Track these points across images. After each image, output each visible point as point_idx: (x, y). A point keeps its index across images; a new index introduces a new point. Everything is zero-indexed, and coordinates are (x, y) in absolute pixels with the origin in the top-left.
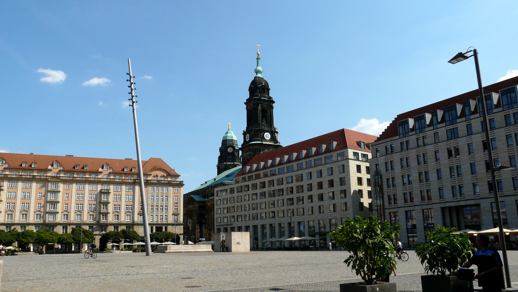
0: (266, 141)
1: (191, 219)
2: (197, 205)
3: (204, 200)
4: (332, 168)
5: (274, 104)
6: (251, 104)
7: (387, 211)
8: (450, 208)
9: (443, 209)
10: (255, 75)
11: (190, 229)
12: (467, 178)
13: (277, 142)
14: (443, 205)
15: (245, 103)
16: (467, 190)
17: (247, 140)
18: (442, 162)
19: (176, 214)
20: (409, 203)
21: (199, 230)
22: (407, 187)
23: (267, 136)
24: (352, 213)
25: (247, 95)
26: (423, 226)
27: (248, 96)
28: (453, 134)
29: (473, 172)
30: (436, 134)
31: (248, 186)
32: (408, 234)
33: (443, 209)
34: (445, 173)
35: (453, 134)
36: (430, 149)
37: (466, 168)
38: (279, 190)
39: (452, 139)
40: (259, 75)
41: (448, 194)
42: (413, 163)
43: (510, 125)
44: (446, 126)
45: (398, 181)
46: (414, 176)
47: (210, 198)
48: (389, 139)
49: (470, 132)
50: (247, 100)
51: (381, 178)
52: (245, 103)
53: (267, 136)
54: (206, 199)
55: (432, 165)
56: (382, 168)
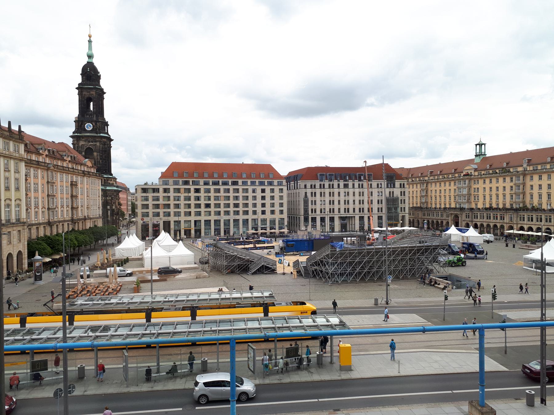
6: (94, 93)
7: (310, 217)
27: (80, 81)
28: (346, 186)
35: (346, 186)
37: (351, 202)
40: (90, 61)
46: (327, 202)
49: (353, 187)
56: (309, 195)
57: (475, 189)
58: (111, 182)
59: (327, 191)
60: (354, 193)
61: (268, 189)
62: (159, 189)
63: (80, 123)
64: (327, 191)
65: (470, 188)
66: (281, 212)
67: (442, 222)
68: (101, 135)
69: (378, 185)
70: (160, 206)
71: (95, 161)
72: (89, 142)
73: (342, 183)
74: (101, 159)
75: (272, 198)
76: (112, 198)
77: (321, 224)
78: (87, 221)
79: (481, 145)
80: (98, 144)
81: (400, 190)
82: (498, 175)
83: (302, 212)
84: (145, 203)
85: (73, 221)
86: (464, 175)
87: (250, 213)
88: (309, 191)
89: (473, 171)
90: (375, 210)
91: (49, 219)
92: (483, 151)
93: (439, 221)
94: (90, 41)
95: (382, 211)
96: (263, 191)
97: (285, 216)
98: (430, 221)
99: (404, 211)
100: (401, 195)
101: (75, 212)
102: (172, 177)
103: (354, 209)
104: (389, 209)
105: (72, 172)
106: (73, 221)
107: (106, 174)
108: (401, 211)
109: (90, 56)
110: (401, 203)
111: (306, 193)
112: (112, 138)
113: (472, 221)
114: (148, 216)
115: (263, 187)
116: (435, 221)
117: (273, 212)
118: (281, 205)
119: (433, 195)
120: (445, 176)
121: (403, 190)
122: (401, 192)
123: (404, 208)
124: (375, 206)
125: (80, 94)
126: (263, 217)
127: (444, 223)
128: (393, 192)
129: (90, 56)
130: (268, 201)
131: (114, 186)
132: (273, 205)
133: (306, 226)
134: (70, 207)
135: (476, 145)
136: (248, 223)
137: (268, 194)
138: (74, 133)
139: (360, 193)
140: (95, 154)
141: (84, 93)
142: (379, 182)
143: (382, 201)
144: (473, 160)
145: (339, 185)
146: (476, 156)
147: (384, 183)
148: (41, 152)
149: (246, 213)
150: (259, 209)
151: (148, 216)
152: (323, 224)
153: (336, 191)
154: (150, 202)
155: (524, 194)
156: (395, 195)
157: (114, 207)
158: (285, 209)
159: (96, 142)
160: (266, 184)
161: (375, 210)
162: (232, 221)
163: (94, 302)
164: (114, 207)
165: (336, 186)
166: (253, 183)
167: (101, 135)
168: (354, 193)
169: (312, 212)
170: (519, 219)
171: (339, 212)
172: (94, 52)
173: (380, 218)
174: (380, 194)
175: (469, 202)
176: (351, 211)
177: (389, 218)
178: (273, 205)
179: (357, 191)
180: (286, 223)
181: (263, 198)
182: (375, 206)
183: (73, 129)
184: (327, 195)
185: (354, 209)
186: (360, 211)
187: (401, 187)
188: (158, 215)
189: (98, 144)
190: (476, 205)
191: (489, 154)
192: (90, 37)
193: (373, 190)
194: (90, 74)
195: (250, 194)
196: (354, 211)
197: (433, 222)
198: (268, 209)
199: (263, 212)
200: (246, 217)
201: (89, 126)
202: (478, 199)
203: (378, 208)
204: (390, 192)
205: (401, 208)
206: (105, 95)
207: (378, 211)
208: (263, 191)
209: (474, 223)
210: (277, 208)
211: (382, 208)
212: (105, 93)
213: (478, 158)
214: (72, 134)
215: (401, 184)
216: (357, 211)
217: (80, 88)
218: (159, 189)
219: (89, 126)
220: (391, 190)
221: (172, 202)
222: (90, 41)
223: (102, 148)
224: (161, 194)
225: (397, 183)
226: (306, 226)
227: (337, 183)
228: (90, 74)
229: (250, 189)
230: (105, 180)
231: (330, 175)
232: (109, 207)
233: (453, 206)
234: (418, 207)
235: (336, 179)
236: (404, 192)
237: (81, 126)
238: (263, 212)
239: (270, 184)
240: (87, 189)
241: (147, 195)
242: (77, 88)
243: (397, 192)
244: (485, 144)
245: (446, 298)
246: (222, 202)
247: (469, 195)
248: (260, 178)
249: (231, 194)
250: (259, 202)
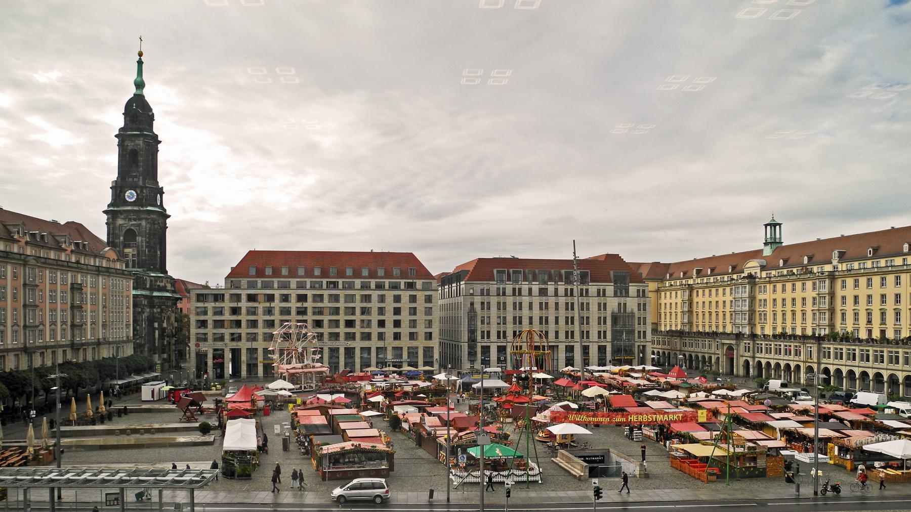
7: (479, 345)
13: (165, 210)
18: (534, 312)
19: (128, 326)
20: (502, 340)
28: (543, 292)
29: (557, 322)
30: (530, 290)
34: (536, 320)
35: (543, 292)
37: (552, 319)
42: (510, 308)
46: (510, 319)
49: (556, 294)
55: (525, 312)
56: (478, 307)
57: (760, 300)
58: (162, 284)
59: (510, 300)
60: (557, 304)
61: (405, 295)
62: (223, 295)
63: (118, 189)
64: (510, 300)
65: (752, 298)
66: (429, 336)
67: (710, 358)
68: (149, 208)
69: (599, 291)
70: (226, 324)
71: (138, 251)
72: (130, 220)
73: (536, 288)
74: (147, 247)
75: (413, 311)
76: (162, 310)
77: (499, 359)
78: (101, 346)
79: (774, 225)
80: (144, 223)
81: (636, 300)
82: (794, 277)
83: (465, 337)
84: (202, 318)
85: (75, 347)
86: (744, 277)
87: (374, 336)
88: (478, 300)
89: (758, 271)
90: (594, 336)
91: (25, 343)
92: (778, 236)
93: (707, 356)
95: (605, 337)
96: (397, 299)
97: (435, 343)
98: (687, 354)
99: (645, 337)
100: (639, 310)
101: (77, 332)
102: (246, 275)
103: (557, 332)
104: (616, 335)
105: (77, 267)
106: (75, 347)
107: (154, 272)
108: (639, 337)
110: (639, 324)
112: (168, 213)
113: (754, 358)
114: (205, 340)
115: (397, 293)
116: (700, 355)
117: (412, 336)
119: (700, 310)
120: (719, 277)
121: (642, 301)
122: (639, 305)
123: (645, 332)
124: (594, 329)
125: (121, 145)
126: (397, 343)
127: (713, 360)
128: (625, 304)
130: (405, 317)
131: (167, 291)
132: (413, 323)
133: (472, 361)
134: (69, 324)
135: (766, 225)
136: (369, 354)
137: (405, 304)
138: (109, 206)
139: (567, 304)
140: (139, 239)
141: (126, 143)
142: (602, 286)
143: (605, 318)
144: (761, 251)
145: (530, 290)
146: (766, 244)
147: (610, 289)
148: (16, 237)
149: (367, 337)
150: (389, 330)
151: (205, 340)
152: (502, 358)
153: (526, 300)
154: (210, 318)
155: (832, 311)
156: (628, 310)
157: (165, 325)
158: (435, 330)
159: (140, 219)
160: (402, 287)
161: (594, 336)
162: (342, 351)
163: (141, 478)
164: (165, 325)
165: (525, 291)
166: (379, 287)
167: (149, 208)
168: (557, 304)
169: (483, 337)
170: (822, 355)
173: (602, 349)
174: (602, 307)
175: (752, 324)
176: (552, 336)
177: (616, 351)
178: (413, 323)
179: (562, 301)
180: (436, 356)
181: (397, 311)
182: (594, 329)
183: (109, 199)
184: (510, 308)
185: (557, 332)
187: (638, 296)
188: (221, 338)
189: (144, 223)
190: (762, 328)
191: (786, 242)
193: (591, 300)
194: (138, 114)
195: (374, 305)
196: (557, 337)
197: (697, 357)
198: (405, 330)
199: (397, 336)
200: (366, 344)
201: (131, 195)
202: (765, 319)
203: (599, 332)
204: (619, 304)
205: (639, 332)
206: (159, 146)
207: (599, 337)
208: (397, 299)
209: (757, 360)
210: (421, 329)
211: (605, 332)
212: (160, 142)
213: (768, 247)
214: (106, 208)
215: (638, 291)
216: (562, 336)
217: (122, 136)
218: (223, 295)
219: (131, 195)
220: (622, 300)
221: (244, 318)
223: (150, 229)
224: (227, 305)
225: (633, 289)
226: (472, 361)
228: (138, 114)
229: (375, 294)
230: (151, 281)
231: (514, 272)
232: (156, 325)
233: (728, 330)
234: (676, 331)
235: (525, 279)
236: (645, 305)
237: (119, 196)
238: (397, 336)
239: (410, 286)
240: (104, 294)
241: (206, 305)
242: (116, 136)
243: (632, 304)
244: (780, 225)
245: (598, 492)
246: (326, 318)
247: (752, 312)
248: (376, 277)
249: (342, 305)
250: (389, 318)
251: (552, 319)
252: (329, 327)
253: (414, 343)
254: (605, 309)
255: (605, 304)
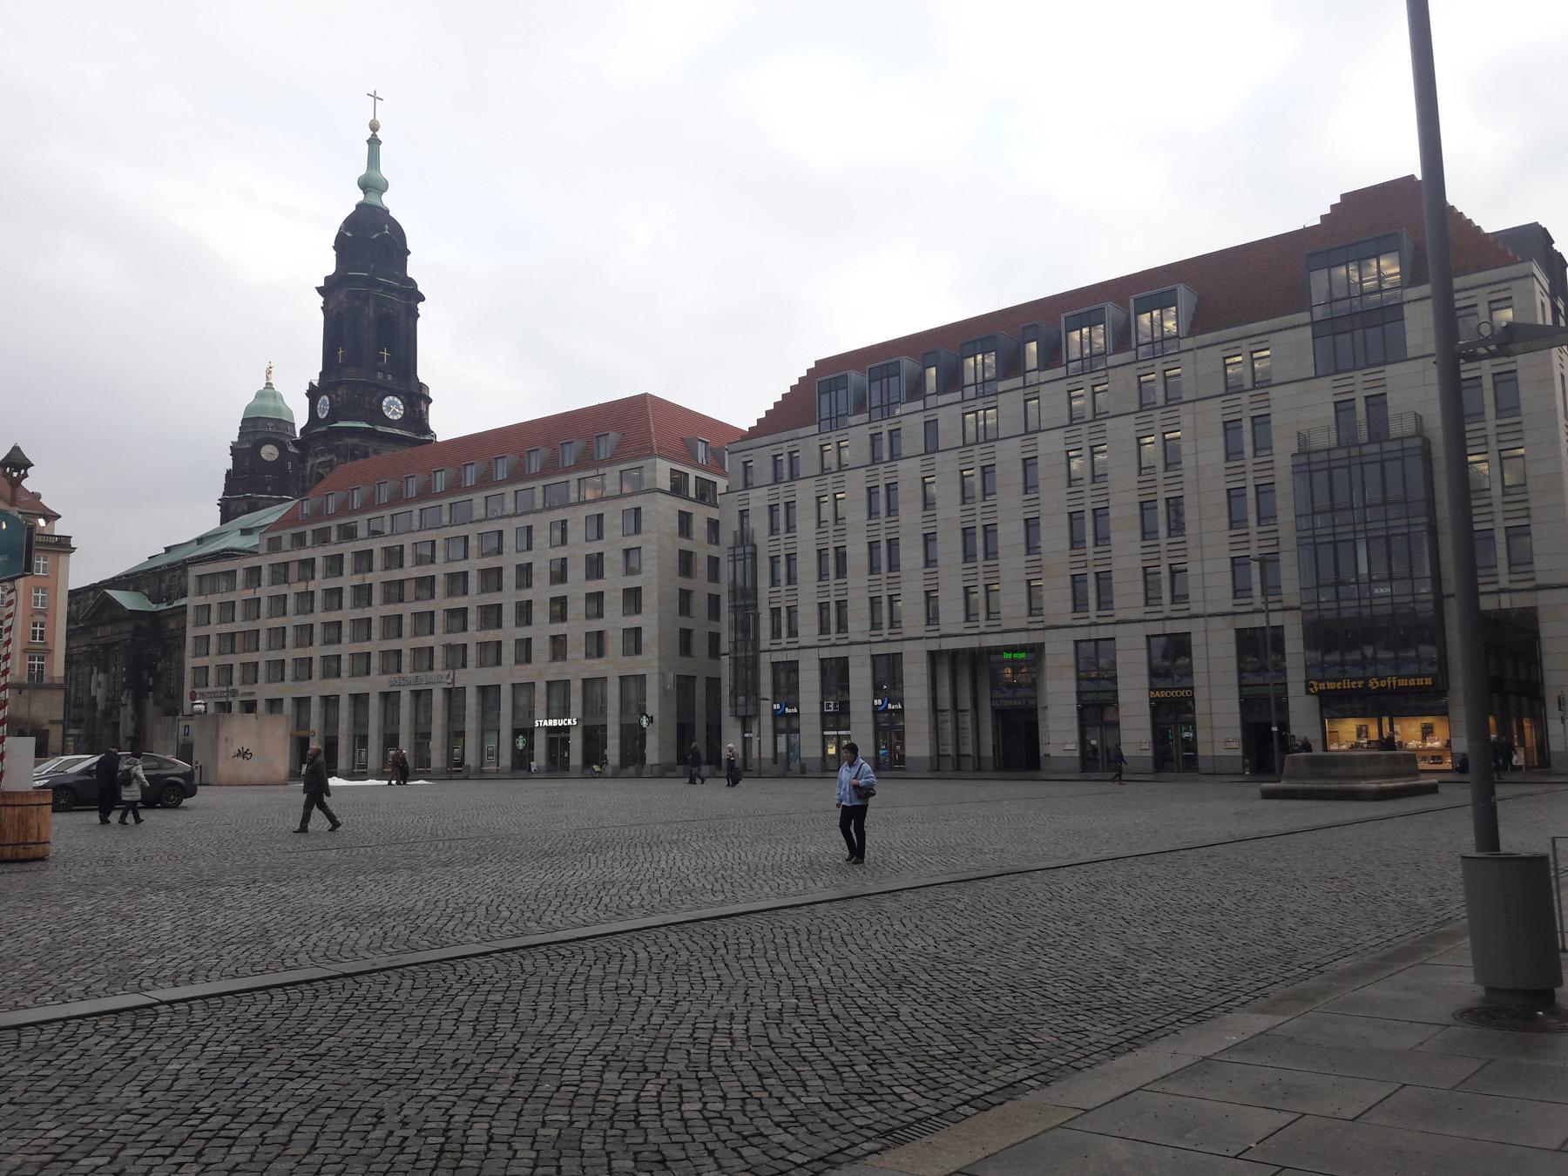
0: (391, 423)
1: (105, 671)
2: (128, 627)
3: (154, 607)
4: (600, 516)
5: (420, 305)
6: (342, 296)
7: (765, 661)
8: (954, 654)
9: (933, 656)
10: (359, 196)
11: (101, 707)
12: (1012, 561)
14: (934, 645)
15: (320, 290)
16: (1012, 605)
17: (322, 416)
18: (941, 514)
21: (130, 710)
22: (832, 587)
23: (393, 408)
24: (656, 663)
25: (329, 266)
26: (870, 708)
27: (331, 269)
30: (931, 427)
31: (309, 564)
32: (824, 729)
33: (933, 656)
36: (908, 471)
37: (1010, 534)
38: (420, 581)
39: (977, 443)
40: (373, 200)
41: (951, 613)
43: (1153, 406)
44: (963, 401)
45: (807, 566)
46: (857, 554)
47: (176, 604)
48: (785, 435)
50: (327, 279)
51: (754, 555)
52: (320, 290)
53: (393, 408)
54: (163, 607)
56: (759, 524)
66: (634, 640)
94: (374, 143)
97: (649, 663)
109: (372, 184)
111: (743, 514)
118: (633, 598)
128: (1377, 402)
129: (372, 184)
133: (745, 722)
143: (1265, 490)
145: (931, 427)
171: (932, 617)
172: (386, 170)
186: (1079, 604)
192: (374, 127)
204: (1343, 407)
220: (1359, 384)
222: (374, 143)
227: (919, 419)
251: (1010, 534)
252: (384, 637)
253: (596, 667)
254: (1262, 445)
255: (1261, 422)
